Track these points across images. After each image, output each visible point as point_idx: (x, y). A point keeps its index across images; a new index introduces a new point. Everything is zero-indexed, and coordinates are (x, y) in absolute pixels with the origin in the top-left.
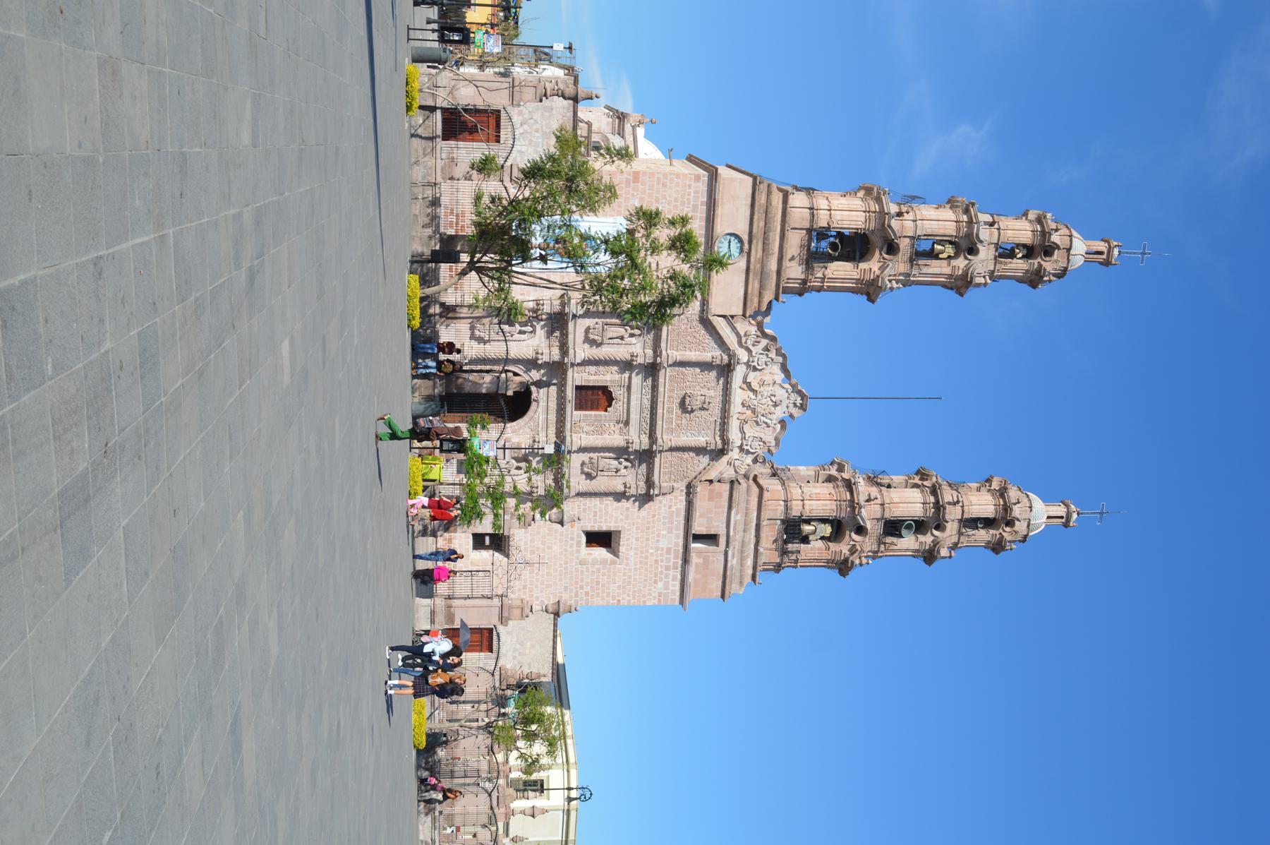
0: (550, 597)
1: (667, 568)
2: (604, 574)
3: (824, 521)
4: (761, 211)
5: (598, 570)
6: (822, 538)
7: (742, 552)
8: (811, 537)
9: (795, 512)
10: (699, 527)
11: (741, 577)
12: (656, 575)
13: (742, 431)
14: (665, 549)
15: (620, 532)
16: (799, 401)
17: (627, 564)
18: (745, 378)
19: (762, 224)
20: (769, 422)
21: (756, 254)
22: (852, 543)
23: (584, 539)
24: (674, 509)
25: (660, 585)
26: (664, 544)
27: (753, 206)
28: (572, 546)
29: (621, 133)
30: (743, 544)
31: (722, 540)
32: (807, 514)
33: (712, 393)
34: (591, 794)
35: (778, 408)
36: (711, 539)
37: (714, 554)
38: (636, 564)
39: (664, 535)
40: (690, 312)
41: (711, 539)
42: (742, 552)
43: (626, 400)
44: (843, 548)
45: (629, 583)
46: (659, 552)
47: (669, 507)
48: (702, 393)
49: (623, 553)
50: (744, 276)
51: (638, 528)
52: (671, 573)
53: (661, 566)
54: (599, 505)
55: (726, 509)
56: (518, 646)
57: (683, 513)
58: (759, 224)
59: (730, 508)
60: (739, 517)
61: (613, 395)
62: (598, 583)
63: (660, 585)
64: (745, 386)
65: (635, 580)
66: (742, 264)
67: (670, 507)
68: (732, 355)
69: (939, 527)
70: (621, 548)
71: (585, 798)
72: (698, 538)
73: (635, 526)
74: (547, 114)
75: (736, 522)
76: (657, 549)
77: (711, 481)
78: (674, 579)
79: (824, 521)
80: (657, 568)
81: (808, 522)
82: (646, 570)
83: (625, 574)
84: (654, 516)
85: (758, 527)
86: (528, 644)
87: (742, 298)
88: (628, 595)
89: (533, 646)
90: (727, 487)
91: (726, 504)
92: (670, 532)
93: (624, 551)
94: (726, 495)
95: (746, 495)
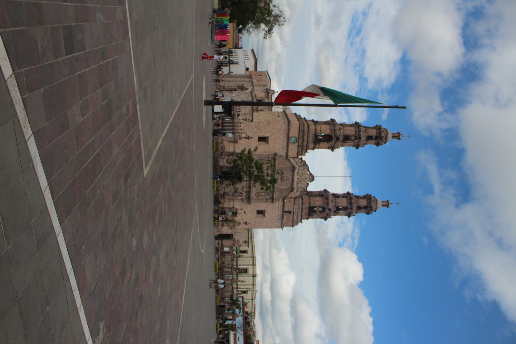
1: (278, 220)
2: (261, 221)
3: (320, 207)
4: (302, 131)
5: (260, 220)
6: (320, 211)
7: (297, 215)
8: (317, 211)
9: (312, 205)
10: (286, 209)
13: (297, 185)
15: (265, 211)
16: (312, 178)
18: (298, 172)
19: (302, 134)
21: (301, 141)
22: (327, 213)
23: (256, 212)
24: (279, 205)
25: (276, 224)
26: (277, 214)
27: (299, 130)
28: (253, 214)
29: (268, 98)
30: (298, 213)
31: (292, 213)
32: (315, 206)
33: (289, 176)
36: (290, 212)
37: (290, 216)
39: (277, 212)
41: (290, 212)
42: (297, 215)
44: (325, 214)
46: (276, 216)
47: (278, 204)
48: (287, 176)
50: (297, 147)
52: (279, 221)
55: (293, 205)
57: (282, 206)
58: (301, 134)
59: (294, 205)
60: (297, 207)
62: (260, 223)
63: (276, 224)
64: (298, 175)
66: (297, 144)
67: (278, 204)
68: (294, 167)
69: (352, 209)
72: (286, 212)
74: (245, 109)
75: (296, 208)
76: (275, 215)
77: (289, 198)
78: (280, 222)
79: (320, 207)
81: (315, 207)
84: (274, 207)
85: (302, 209)
90: (293, 199)
91: (293, 204)
92: (278, 210)
94: (293, 201)
95: (299, 202)
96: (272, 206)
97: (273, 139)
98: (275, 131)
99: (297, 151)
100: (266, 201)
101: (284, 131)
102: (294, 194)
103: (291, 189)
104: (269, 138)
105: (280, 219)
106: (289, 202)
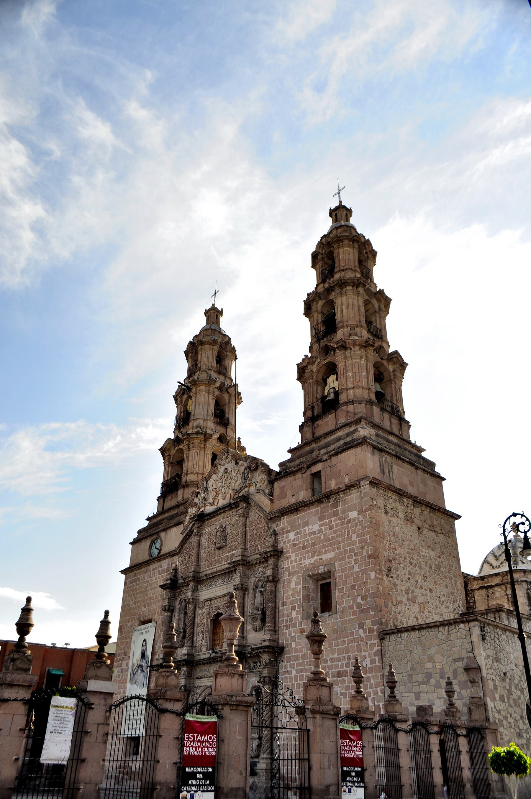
0: (371, 645)
11: (348, 435)
12: (343, 523)
14: (321, 523)
17: (335, 558)
20: (236, 472)
31: (315, 469)
34: (515, 515)
35: (230, 469)
38: (333, 550)
40: (178, 564)
43: (219, 600)
45: (352, 550)
46: (323, 528)
49: (324, 568)
50: (168, 531)
51: (304, 559)
53: (335, 521)
54: (287, 606)
56: (433, 681)
57: (293, 517)
61: (215, 613)
62: (353, 587)
65: (349, 545)
66: (163, 535)
70: (321, 571)
71: (523, 523)
73: (303, 562)
80: (337, 525)
82: (339, 536)
83: (344, 559)
84: (295, 545)
86: (429, 665)
87: (177, 527)
88: (363, 548)
89: (431, 659)
92: (306, 524)
93: (322, 567)
96: (293, 558)
97: (145, 607)
98: (133, 606)
99: (174, 529)
100: (275, 580)
101: (136, 581)
102: (258, 491)
103: (243, 505)
104: (142, 619)
105: (335, 506)
106: (283, 495)
